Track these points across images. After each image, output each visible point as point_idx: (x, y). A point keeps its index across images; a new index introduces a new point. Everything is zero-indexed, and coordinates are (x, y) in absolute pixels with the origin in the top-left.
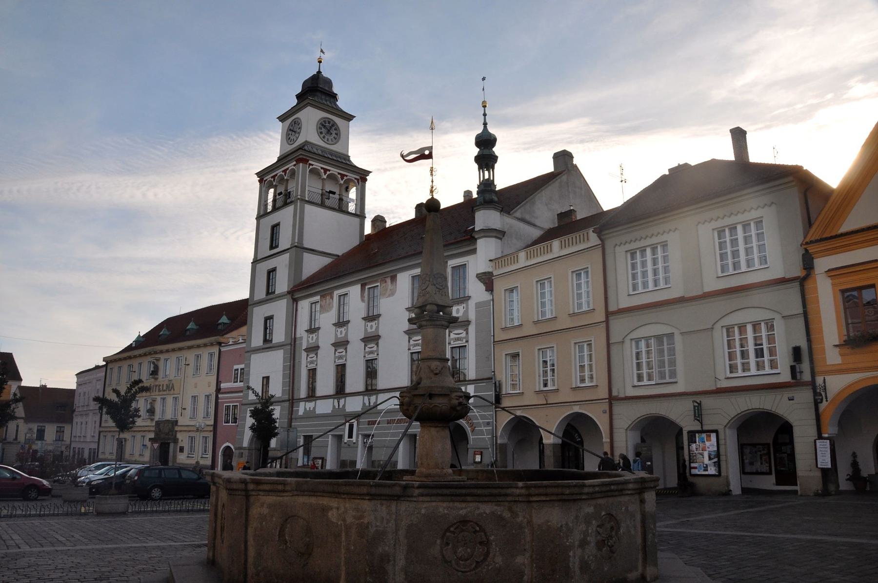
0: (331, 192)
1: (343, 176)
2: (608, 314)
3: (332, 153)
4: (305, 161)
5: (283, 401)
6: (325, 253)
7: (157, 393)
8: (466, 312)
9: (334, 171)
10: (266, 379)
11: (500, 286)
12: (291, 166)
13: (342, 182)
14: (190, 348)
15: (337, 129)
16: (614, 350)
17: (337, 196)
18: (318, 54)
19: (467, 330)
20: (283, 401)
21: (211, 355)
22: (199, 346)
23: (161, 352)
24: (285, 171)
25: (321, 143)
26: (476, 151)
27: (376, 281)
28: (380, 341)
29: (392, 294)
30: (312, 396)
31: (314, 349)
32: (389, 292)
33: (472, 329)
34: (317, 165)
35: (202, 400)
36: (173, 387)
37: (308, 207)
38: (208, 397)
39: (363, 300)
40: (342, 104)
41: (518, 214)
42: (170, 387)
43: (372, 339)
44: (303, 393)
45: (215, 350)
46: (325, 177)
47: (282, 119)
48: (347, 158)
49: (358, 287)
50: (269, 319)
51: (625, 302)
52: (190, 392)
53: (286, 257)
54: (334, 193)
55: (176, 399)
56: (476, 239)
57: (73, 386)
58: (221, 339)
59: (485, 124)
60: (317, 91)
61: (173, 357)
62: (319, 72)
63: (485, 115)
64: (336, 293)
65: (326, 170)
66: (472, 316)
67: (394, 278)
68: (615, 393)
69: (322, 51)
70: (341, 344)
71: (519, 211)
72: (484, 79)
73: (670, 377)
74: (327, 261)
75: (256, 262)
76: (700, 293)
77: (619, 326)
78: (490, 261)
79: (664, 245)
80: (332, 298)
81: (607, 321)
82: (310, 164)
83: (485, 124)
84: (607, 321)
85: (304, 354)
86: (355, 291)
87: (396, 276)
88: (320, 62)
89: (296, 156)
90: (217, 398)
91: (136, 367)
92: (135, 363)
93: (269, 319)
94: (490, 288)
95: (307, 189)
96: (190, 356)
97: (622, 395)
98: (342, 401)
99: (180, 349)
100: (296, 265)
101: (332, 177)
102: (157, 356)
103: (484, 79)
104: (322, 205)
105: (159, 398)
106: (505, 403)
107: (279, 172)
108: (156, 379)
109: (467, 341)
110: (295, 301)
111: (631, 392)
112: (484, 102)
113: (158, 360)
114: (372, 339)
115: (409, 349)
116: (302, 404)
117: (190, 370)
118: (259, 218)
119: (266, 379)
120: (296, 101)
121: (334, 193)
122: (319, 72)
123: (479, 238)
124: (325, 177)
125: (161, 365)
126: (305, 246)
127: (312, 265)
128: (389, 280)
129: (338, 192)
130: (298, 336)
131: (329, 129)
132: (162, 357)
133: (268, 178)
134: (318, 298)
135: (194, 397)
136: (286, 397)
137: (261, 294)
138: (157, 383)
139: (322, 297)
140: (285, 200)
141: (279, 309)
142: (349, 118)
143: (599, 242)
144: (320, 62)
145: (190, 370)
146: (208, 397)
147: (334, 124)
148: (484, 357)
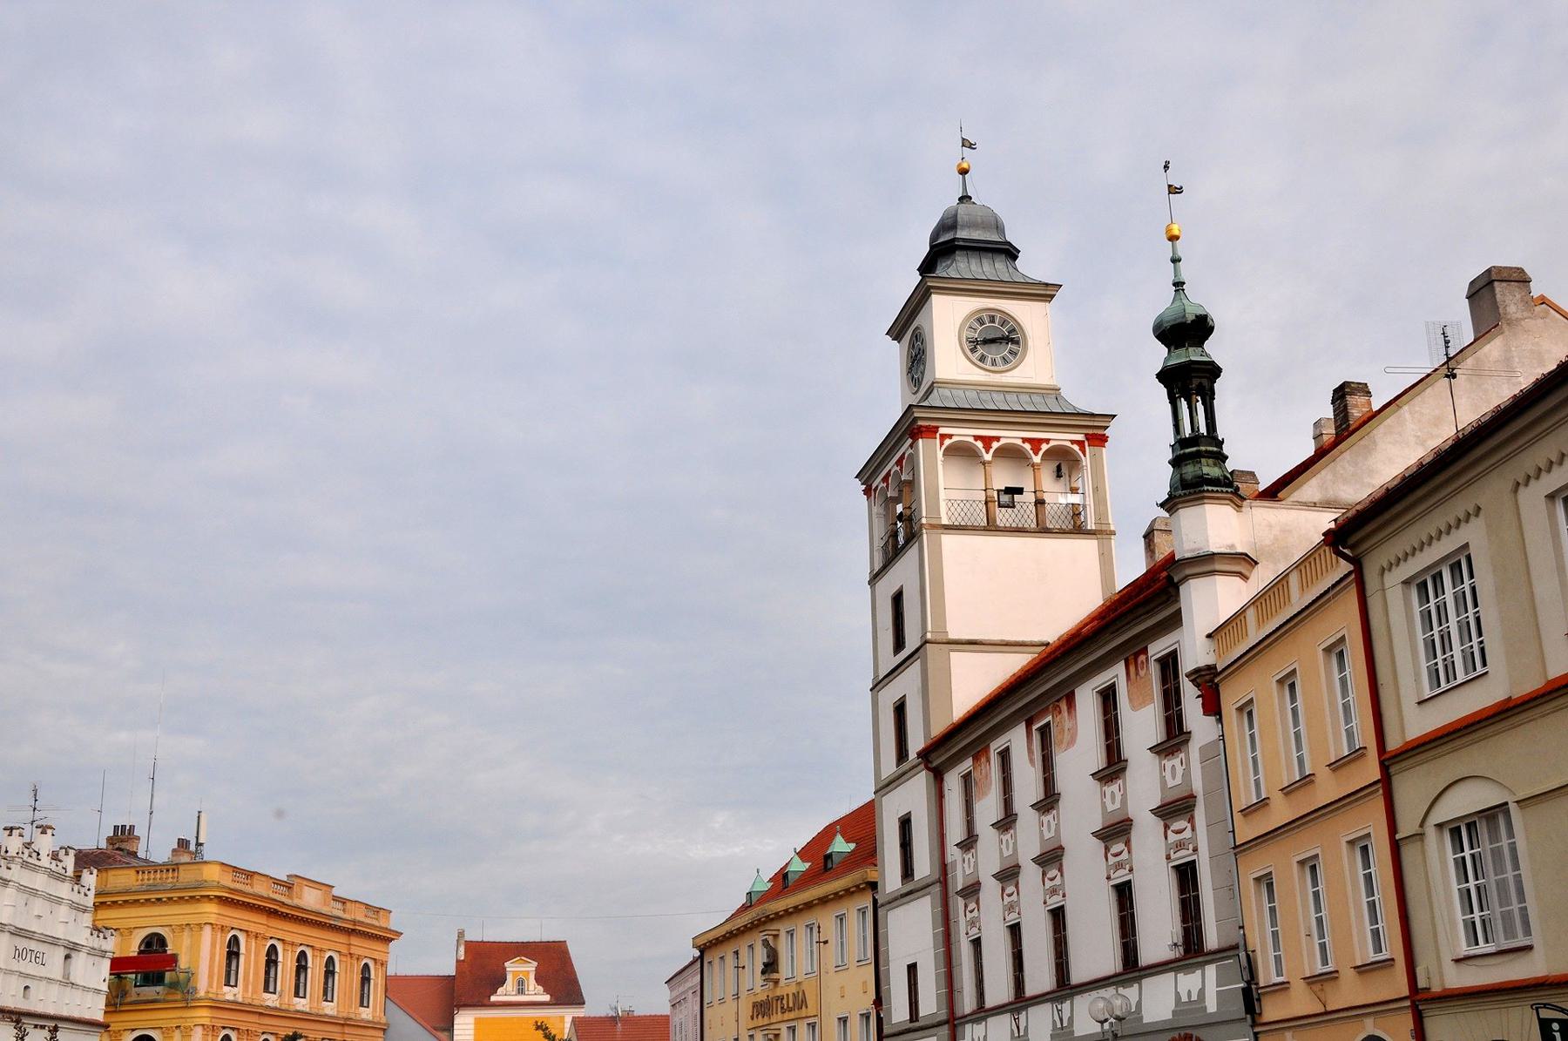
0: (1013, 491)
1: (1037, 444)
2: (1388, 762)
3: (1005, 390)
4: (932, 431)
5: (939, 1024)
6: (1008, 644)
7: (779, 1017)
8: (1187, 774)
9: (1011, 436)
10: (912, 968)
11: (1231, 698)
12: (905, 447)
13: (1037, 459)
14: (824, 901)
16: (1409, 854)
17: (1028, 498)
19: (1191, 820)
20: (939, 1024)
21: (863, 911)
22: (838, 897)
23: (778, 917)
24: (899, 463)
25: (976, 375)
26: (1158, 355)
27: (1044, 712)
28: (1066, 861)
29: (1072, 742)
30: (983, 1013)
31: (972, 891)
32: (1067, 737)
33: (1200, 813)
34: (963, 434)
35: (855, 1024)
36: (804, 1001)
37: (949, 541)
38: (867, 1016)
39: (1032, 761)
40: (1030, 266)
42: (800, 1002)
43: (1051, 858)
44: (967, 1004)
45: (866, 901)
46: (988, 457)
47: (896, 332)
49: (1021, 729)
50: (905, 823)
51: (1413, 723)
52: (834, 1008)
53: (915, 668)
54: (1020, 491)
55: (812, 1026)
56: (1176, 587)
57: (664, 1009)
58: (872, 875)
59: (1179, 285)
60: (961, 248)
61: (799, 924)
62: (965, 198)
63: (1175, 261)
64: (996, 746)
65: (987, 441)
66: (1198, 786)
67: (1070, 699)
68: (1422, 984)
69: (967, 144)
70: (1009, 875)
71: (1314, 482)
72: (1166, 167)
73: (1509, 932)
74: (1016, 663)
75: (877, 686)
76: (1531, 684)
77: (1412, 789)
78: (1209, 636)
79: (1460, 563)
80: (988, 760)
81: (1386, 782)
82: (943, 437)
83: (1179, 285)
84: (1386, 782)
85: (961, 902)
86: (1017, 739)
87: (1073, 693)
88: (964, 172)
90: (880, 1021)
91: (744, 952)
92: (742, 945)
93: (905, 823)
94: (1212, 706)
95: (943, 495)
96: (826, 920)
97: (1436, 988)
98: (1023, 1016)
99: (809, 906)
101: (1010, 454)
102: (775, 926)
103: (1166, 167)
104: (991, 528)
105: (784, 1027)
106: (1272, 1010)
107: (891, 465)
108: (776, 982)
109: (1195, 850)
110: (938, 775)
111: (1458, 978)
112: (1168, 230)
113: (776, 936)
114: (1051, 858)
115: (1108, 878)
116: (968, 1027)
117: (831, 954)
118: (875, 578)
119: (912, 968)
121: (1020, 491)
122: (965, 198)
123: (1186, 578)
124: (988, 457)
125: (783, 947)
126: (952, 636)
127: (971, 682)
128: (1064, 706)
129: (1028, 486)
130: (949, 859)
131: (998, 340)
132: (783, 927)
133: (877, 481)
134: (967, 765)
135: (844, 1021)
136: (943, 1015)
137: (890, 767)
138: (778, 993)
139: (976, 758)
140: (901, 535)
141: (914, 795)
142: (1044, 292)
143: (1351, 567)
144: (964, 172)
146: (867, 1016)
147: (1006, 319)
148: (1230, 891)
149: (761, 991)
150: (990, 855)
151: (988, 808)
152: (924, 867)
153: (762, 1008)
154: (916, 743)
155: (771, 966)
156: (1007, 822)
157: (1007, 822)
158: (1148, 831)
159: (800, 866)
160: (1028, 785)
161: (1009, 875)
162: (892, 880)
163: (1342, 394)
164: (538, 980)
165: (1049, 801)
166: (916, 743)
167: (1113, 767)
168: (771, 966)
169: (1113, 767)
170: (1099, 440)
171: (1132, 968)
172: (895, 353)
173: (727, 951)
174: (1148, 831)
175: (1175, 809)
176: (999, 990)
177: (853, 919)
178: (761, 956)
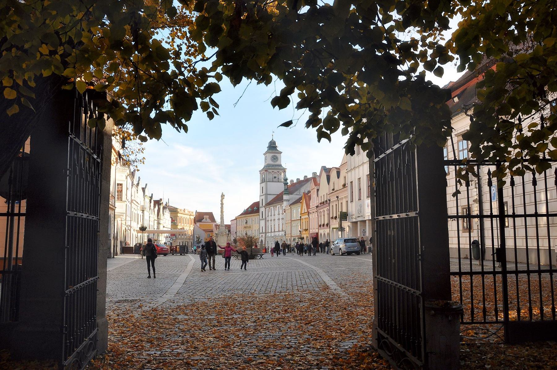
9: (276, 171)
15: (277, 158)
18: (272, 133)
25: (272, 163)
41: (295, 194)
42: (250, 227)
48: (281, 166)
51: (293, 219)
70: (271, 220)
89: (267, 169)
92: (243, 219)
100: (266, 198)
104: (273, 181)
117: (254, 222)
120: (266, 149)
127: (270, 198)
131: (275, 158)
145: (254, 222)
149: (245, 225)
150: (269, 218)
151: (270, 214)
152: (264, 217)
153: (245, 227)
154: (264, 205)
155: (246, 223)
156: (271, 216)
157: (271, 216)
158: (281, 220)
159: (250, 209)
160: (273, 214)
161: (271, 220)
162: (261, 218)
163: (305, 176)
164: (209, 218)
165: (274, 215)
166: (264, 205)
167: (279, 214)
168: (246, 223)
169: (279, 214)
170: (285, 171)
171: (279, 231)
172: (264, 156)
173: (240, 219)
174: (281, 220)
175: (283, 219)
176: (270, 231)
177: (257, 219)
178: (245, 221)
